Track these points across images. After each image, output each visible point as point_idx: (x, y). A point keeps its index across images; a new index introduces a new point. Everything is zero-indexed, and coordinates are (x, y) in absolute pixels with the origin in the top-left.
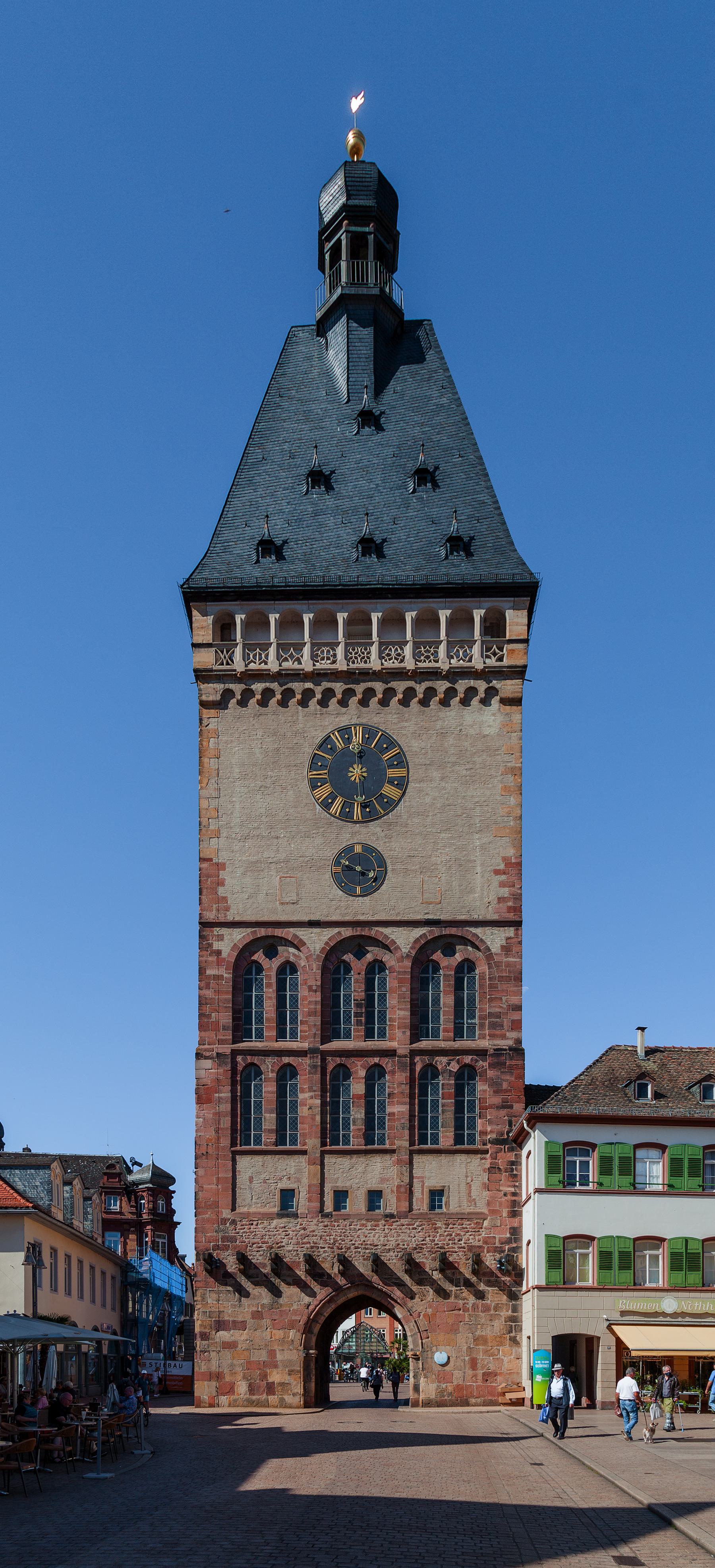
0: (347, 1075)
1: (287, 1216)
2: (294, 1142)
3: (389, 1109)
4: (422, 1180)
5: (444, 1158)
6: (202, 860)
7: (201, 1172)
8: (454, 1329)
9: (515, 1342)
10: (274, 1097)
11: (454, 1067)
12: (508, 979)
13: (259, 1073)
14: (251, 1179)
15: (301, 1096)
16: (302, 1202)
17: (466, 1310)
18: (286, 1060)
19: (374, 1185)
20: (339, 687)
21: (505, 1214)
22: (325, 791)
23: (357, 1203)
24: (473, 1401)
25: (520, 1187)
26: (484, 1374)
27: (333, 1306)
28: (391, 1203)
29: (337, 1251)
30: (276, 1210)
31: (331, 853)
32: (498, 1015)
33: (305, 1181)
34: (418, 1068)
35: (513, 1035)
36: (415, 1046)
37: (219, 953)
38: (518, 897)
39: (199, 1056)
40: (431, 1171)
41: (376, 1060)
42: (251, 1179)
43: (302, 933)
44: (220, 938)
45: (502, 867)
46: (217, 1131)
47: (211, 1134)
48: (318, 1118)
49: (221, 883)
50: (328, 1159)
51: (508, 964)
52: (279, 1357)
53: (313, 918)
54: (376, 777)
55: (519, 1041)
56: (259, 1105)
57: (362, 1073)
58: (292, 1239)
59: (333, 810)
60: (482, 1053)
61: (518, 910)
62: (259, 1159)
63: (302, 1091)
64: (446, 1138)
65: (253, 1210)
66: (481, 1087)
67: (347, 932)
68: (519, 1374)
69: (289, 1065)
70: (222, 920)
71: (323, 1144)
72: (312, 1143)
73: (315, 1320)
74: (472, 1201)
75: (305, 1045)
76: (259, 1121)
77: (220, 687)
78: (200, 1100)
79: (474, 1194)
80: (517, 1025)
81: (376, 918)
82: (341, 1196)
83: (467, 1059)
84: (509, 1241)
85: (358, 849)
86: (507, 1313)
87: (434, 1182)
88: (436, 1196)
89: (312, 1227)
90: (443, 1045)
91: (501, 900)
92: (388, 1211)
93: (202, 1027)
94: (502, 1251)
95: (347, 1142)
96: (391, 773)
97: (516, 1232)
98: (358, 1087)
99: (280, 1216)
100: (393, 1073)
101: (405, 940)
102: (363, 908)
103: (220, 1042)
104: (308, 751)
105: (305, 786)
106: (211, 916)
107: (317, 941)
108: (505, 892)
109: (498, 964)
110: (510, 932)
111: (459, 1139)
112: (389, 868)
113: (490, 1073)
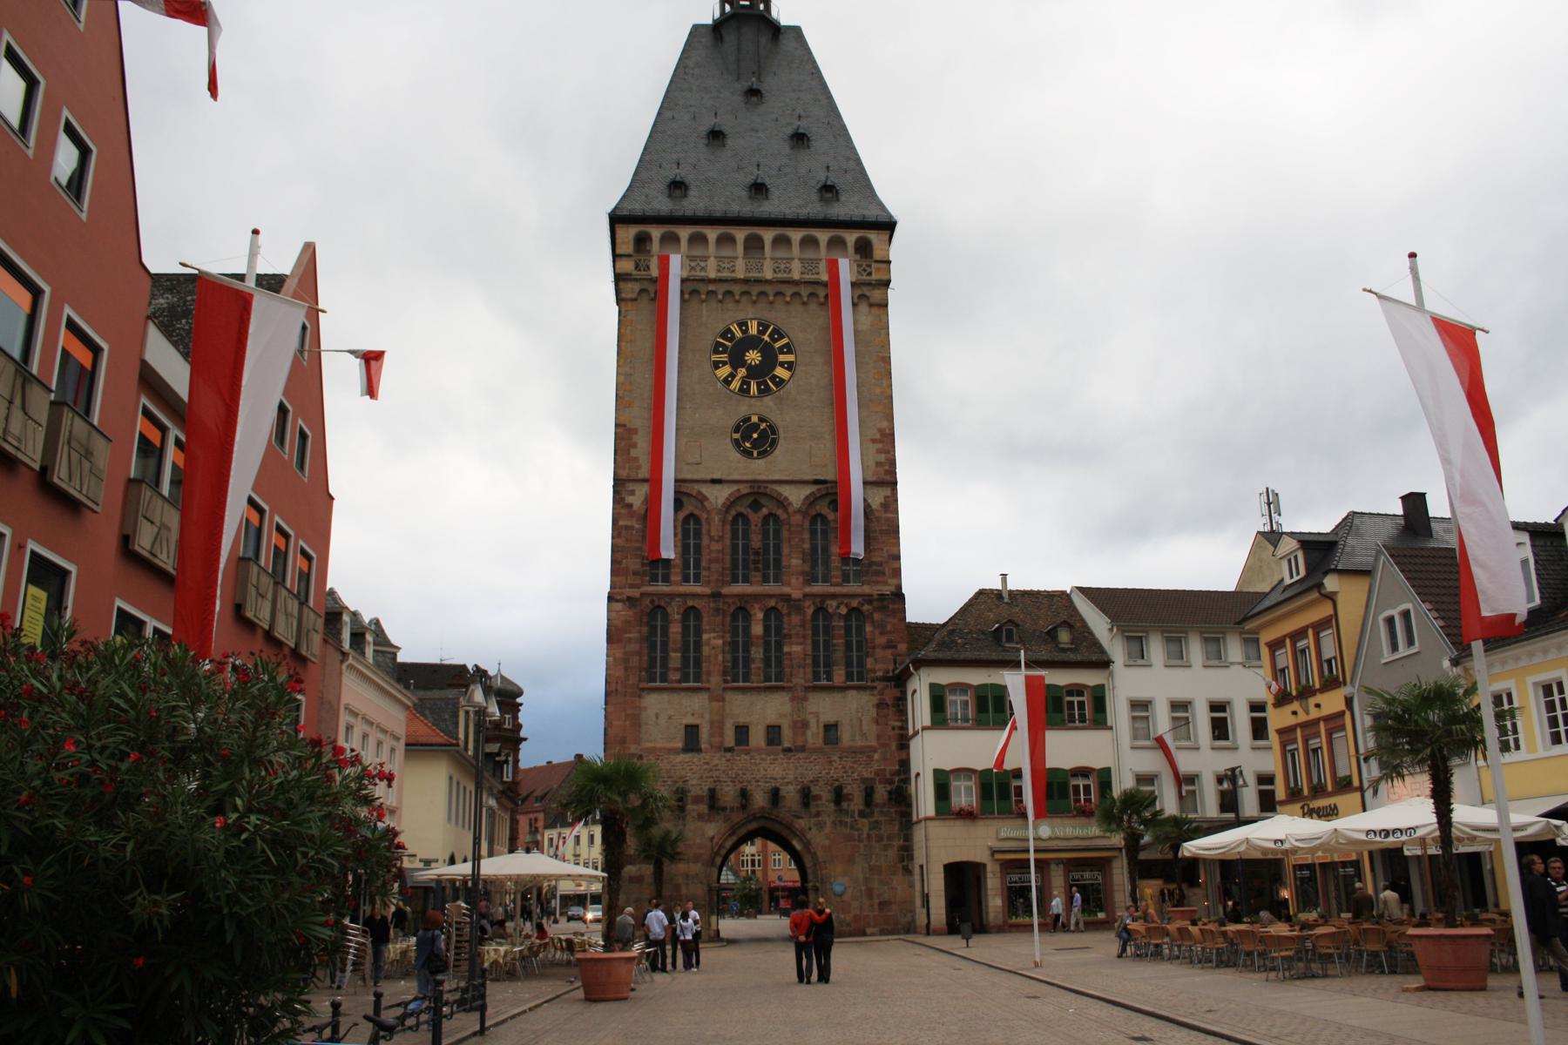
0: (748, 617)
1: (692, 750)
2: (698, 679)
3: (786, 649)
4: (817, 715)
5: (838, 696)
6: (617, 425)
7: (611, 708)
8: (851, 860)
9: (908, 871)
10: (679, 637)
11: (843, 610)
12: (887, 532)
13: (666, 617)
14: (657, 716)
15: (705, 636)
16: (704, 734)
17: (860, 840)
18: (690, 603)
19: (772, 719)
20: (737, 289)
21: (894, 746)
22: (725, 371)
23: (757, 737)
24: (869, 931)
25: (906, 721)
26: (880, 904)
27: (735, 838)
28: (787, 740)
29: (738, 787)
30: (680, 745)
31: (732, 422)
32: (880, 564)
33: (707, 716)
34: (810, 611)
35: (894, 581)
36: (808, 590)
37: (631, 506)
38: (893, 463)
39: (611, 598)
40: (824, 707)
41: (772, 603)
42: (657, 716)
43: (706, 490)
44: (632, 493)
45: (878, 436)
46: (626, 669)
47: (620, 672)
48: (720, 657)
49: (635, 446)
50: (729, 696)
51: (887, 519)
52: (684, 891)
53: (716, 476)
54: (770, 359)
55: (899, 587)
56: (665, 644)
57: (760, 615)
58: (693, 772)
59: (732, 387)
60: (868, 599)
61: (892, 472)
62: (665, 696)
63: (708, 632)
64: (839, 675)
65: (659, 745)
66: (868, 628)
67: (745, 489)
68: (913, 902)
69: (693, 607)
70: (633, 475)
71: (726, 681)
72: (715, 680)
73: (717, 854)
74: (864, 735)
75: (707, 590)
76: (665, 660)
77: (637, 287)
78: (610, 640)
79: (865, 727)
80: (897, 573)
81: (770, 478)
82: (742, 732)
83: (855, 604)
84: (898, 773)
85: (755, 419)
86: (898, 843)
87: (829, 717)
88: (831, 729)
89: (716, 762)
90: (832, 590)
91: (878, 464)
92: (786, 744)
93: (614, 572)
94: (891, 782)
95: (746, 678)
96: (782, 358)
97: (905, 764)
98: (757, 629)
99: (686, 750)
100: (789, 615)
101: (796, 496)
102: (759, 469)
103: (632, 586)
104: (710, 338)
105: (708, 367)
106: (623, 474)
107: (718, 496)
108: (882, 458)
109: (878, 519)
110: (888, 492)
111: (849, 676)
112: (782, 434)
113: (876, 616)
